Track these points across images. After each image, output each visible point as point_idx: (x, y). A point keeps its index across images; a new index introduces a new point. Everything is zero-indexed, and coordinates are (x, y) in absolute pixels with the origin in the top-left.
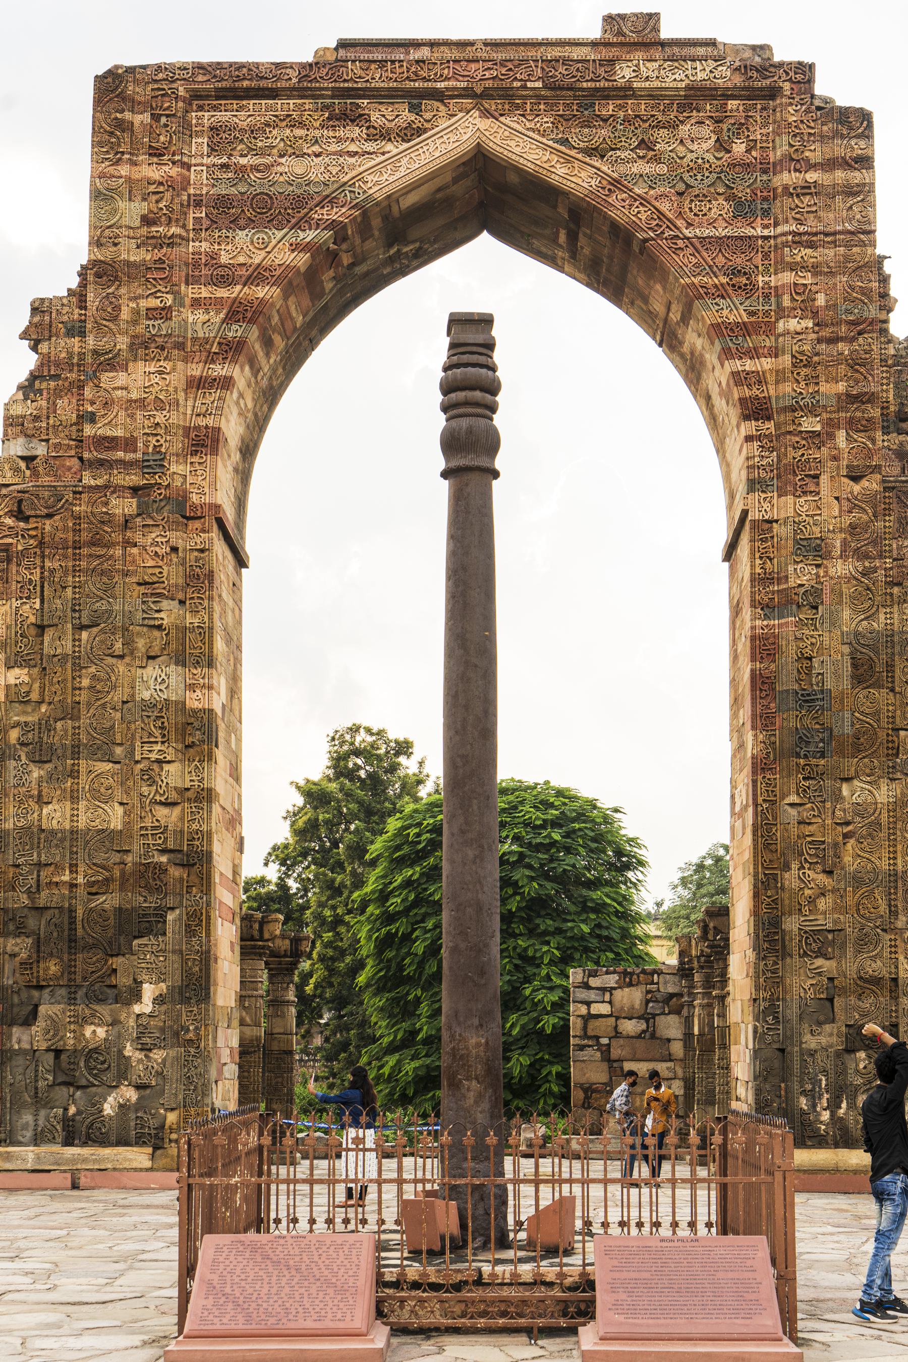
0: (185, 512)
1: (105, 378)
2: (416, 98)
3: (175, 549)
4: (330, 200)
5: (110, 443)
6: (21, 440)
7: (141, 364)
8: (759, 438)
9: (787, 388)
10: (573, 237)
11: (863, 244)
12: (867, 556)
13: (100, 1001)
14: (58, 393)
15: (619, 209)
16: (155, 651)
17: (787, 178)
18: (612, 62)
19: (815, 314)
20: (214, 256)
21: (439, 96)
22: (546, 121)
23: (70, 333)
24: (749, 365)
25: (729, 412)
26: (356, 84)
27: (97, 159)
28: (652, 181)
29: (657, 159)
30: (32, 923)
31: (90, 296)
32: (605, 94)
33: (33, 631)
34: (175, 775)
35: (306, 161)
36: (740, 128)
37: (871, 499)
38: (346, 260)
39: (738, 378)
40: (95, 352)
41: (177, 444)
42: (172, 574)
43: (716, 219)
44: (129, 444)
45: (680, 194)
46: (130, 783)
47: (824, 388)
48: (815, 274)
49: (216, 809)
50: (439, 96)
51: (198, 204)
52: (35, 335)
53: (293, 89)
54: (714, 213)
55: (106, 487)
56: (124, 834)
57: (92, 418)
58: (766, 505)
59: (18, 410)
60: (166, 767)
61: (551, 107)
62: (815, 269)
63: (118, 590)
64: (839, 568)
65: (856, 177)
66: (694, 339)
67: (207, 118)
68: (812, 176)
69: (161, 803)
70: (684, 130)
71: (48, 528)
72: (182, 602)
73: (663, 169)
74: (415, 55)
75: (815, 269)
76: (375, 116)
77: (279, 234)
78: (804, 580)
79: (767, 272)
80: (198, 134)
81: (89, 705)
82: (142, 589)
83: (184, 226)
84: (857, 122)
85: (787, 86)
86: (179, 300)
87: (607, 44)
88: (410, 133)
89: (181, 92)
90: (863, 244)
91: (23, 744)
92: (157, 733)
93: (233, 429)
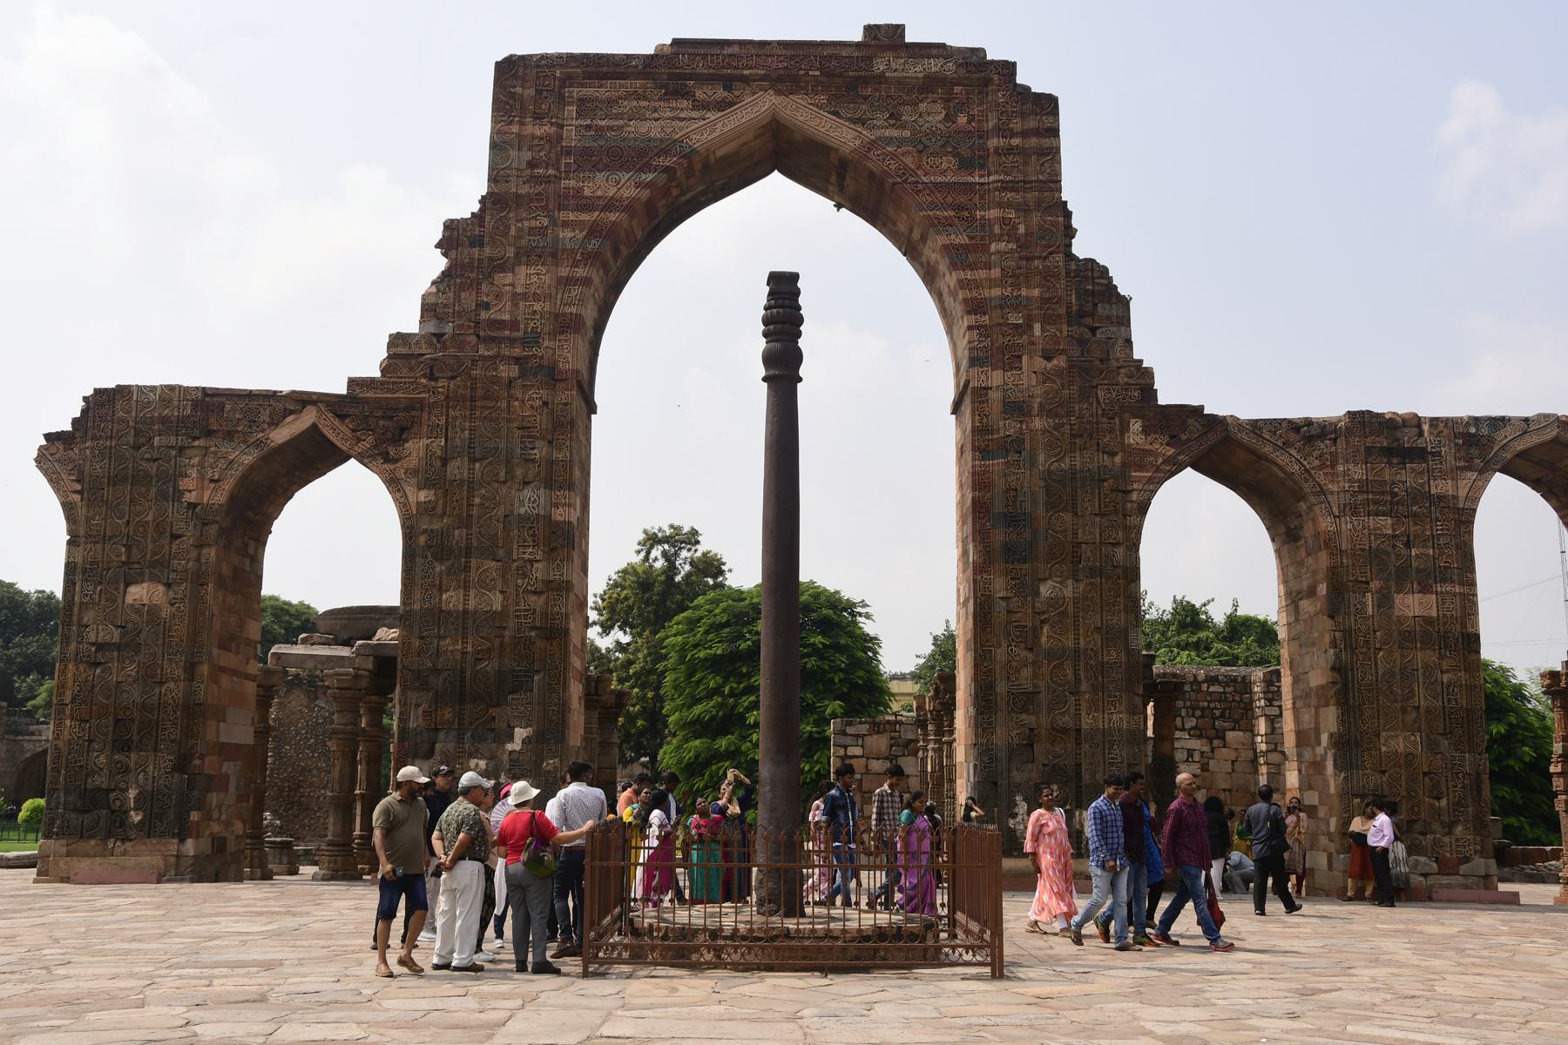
0: (553, 376)
2: (728, 82)
3: (545, 403)
4: (665, 152)
5: (500, 324)
6: (434, 321)
7: (523, 268)
8: (978, 327)
9: (996, 292)
10: (841, 178)
12: (1057, 415)
14: (462, 287)
16: (530, 478)
18: (870, 59)
20: (579, 190)
21: (746, 80)
22: (823, 99)
23: (472, 245)
24: (969, 275)
25: (957, 309)
27: (495, 121)
28: (900, 142)
31: (488, 218)
32: (866, 81)
34: (539, 571)
35: (648, 123)
36: (961, 107)
37: (1059, 372)
38: (675, 192)
39: (963, 284)
40: (491, 259)
42: (542, 421)
43: (946, 170)
44: (514, 325)
45: (920, 152)
48: (1017, 210)
49: (572, 597)
50: (746, 80)
51: (568, 153)
52: (445, 245)
55: (496, 357)
56: (503, 614)
57: (487, 306)
58: (983, 377)
59: (432, 300)
62: (1018, 208)
64: (1037, 423)
65: (1046, 142)
66: (932, 253)
68: (1016, 141)
70: (923, 107)
72: (550, 442)
73: (907, 133)
76: (699, 94)
79: (982, 208)
80: (570, 104)
81: (479, 517)
82: (521, 432)
83: (558, 169)
84: (1048, 104)
85: (996, 77)
86: (554, 222)
88: (722, 106)
91: (430, 547)
93: (590, 314)
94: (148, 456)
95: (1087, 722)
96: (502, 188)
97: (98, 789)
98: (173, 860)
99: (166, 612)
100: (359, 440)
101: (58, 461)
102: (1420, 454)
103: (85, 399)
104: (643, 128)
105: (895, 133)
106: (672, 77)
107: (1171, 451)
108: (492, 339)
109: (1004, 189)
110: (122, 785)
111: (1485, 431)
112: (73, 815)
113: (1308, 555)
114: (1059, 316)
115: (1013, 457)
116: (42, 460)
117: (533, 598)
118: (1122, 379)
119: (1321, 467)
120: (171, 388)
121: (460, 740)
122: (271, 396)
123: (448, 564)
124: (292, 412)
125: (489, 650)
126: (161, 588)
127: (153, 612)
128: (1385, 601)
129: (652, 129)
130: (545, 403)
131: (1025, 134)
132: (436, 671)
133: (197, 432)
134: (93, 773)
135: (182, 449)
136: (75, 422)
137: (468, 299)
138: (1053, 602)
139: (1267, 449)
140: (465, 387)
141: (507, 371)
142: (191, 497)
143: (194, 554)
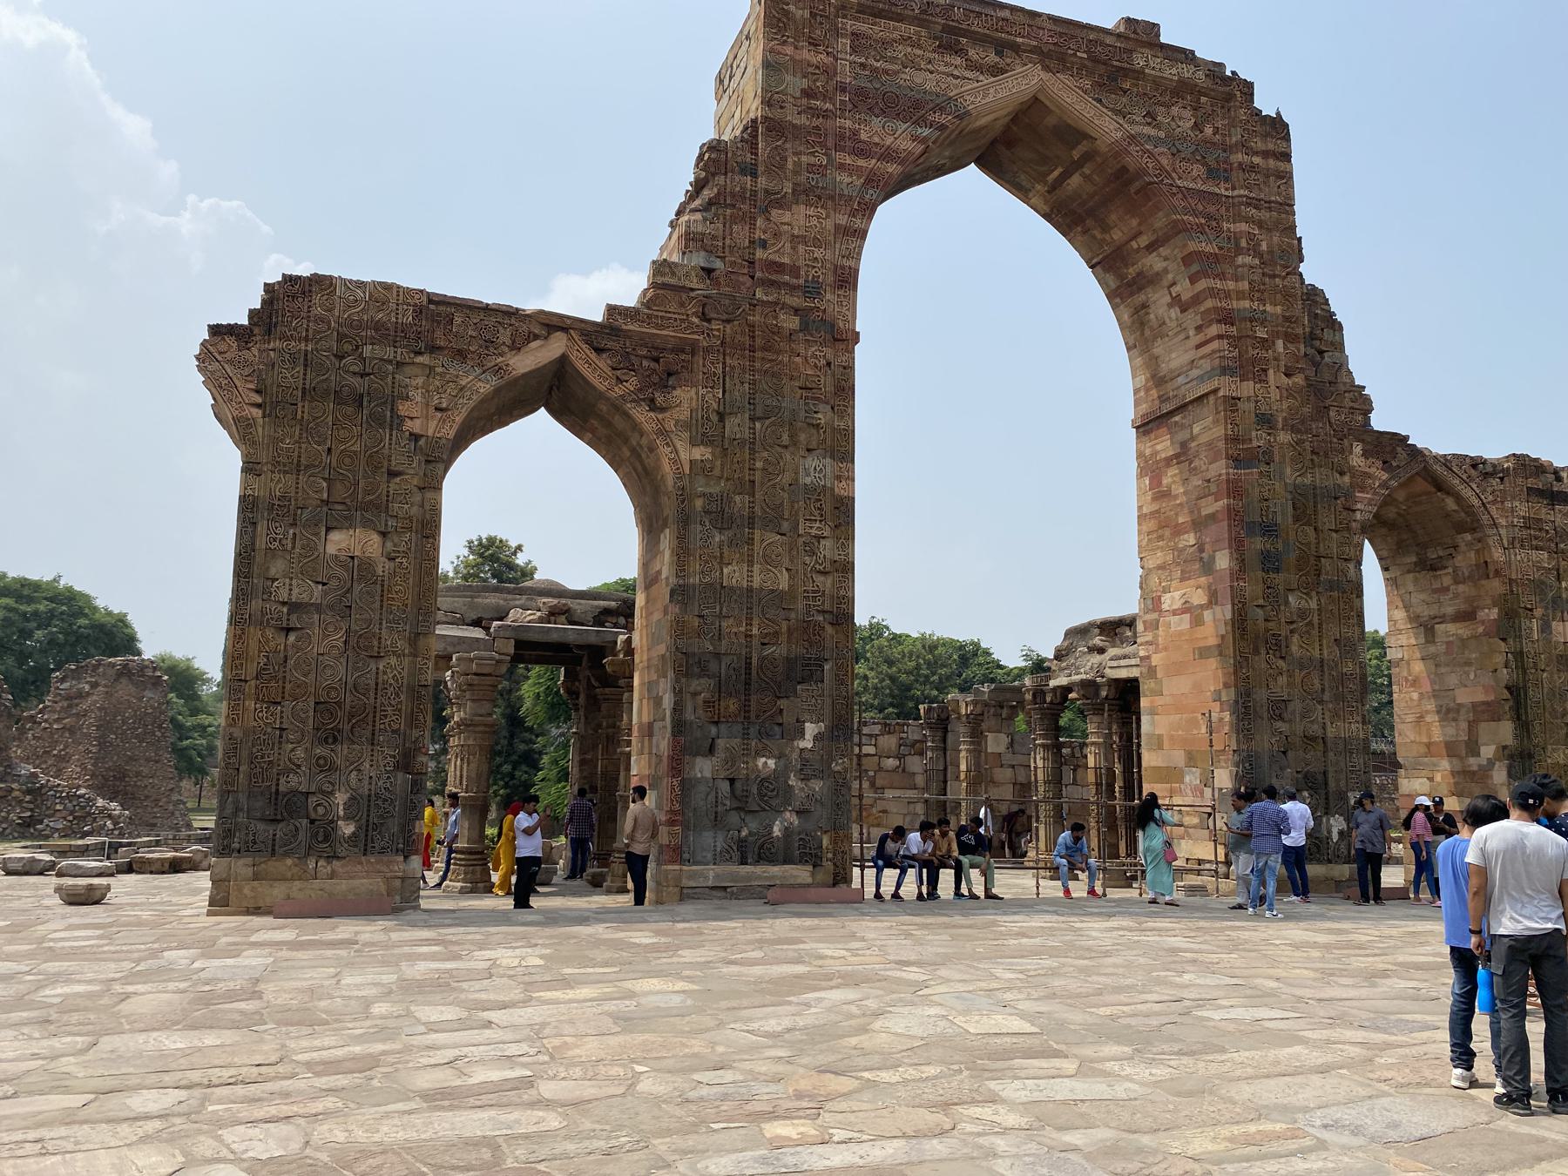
1: (774, 212)
2: (1001, 47)
5: (779, 267)
6: (703, 253)
8: (1228, 337)
9: (1246, 304)
11: (1287, 213)
12: (1299, 431)
14: (734, 220)
16: (814, 445)
17: (1239, 157)
18: (1131, 51)
19: (1261, 256)
20: (855, 133)
21: (1016, 49)
22: (1087, 84)
23: (743, 172)
28: (1157, 142)
29: (1158, 127)
30: (713, 666)
33: (714, 418)
36: (1208, 117)
41: (830, 279)
43: (1193, 177)
44: (794, 271)
47: (1268, 308)
48: (1260, 227)
50: (1016, 49)
51: (843, 90)
53: (916, 18)
54: (1195, 173)
55: (776, 304)
57: (764, 244)
60: (823, 542)
61: (1091, 73)
63: (786, 390)
64: (1284, 437)
65: (1282, 165)
67: (849, 25)
68: (1257, 160)
69: (819, 572)
70: (1175, 110)
71: (728, 330)
73: (1162, 134)
74: (1001, 14)
76: (971, 52)
78: (1261, 443)
88: (996, 71)
90: (1287, 213)
92: (816, 513)
94: (354, 368)
95: (1331, 732)
96: (776, 114)
97: (294, 792)
98: (398, 883)
99: (382, 567)
101: (230, 362)
104: (919, 78)
105: (1147, 130)
107: (1385, 476)
108: (773, 283)
112: (261, 826)
113: (1457, 582)
115: (1264, 468)
116: (206, 358)
117: (819, 579)
118: (1347, 403)
119: (1494, 502)
120: (388, 287)
121: (746, 735)
122: (511, 313)
123: (730, 533)
124: (536, 337)
125: (776, 634)
126: (376, 538)
127: (358, 568)
128: (1546, 628)
129: (927, 81)
130: (829, 364)
131: (1266, 154)
132: (717, 655)
134: (287, 772)
135: (399, 365)
136: (253, 314)
137: (741, 233)
138: (1303, 614)
140: (743, 333)
141: (790, 322)
142: (415, 426)
143: (417, 498)
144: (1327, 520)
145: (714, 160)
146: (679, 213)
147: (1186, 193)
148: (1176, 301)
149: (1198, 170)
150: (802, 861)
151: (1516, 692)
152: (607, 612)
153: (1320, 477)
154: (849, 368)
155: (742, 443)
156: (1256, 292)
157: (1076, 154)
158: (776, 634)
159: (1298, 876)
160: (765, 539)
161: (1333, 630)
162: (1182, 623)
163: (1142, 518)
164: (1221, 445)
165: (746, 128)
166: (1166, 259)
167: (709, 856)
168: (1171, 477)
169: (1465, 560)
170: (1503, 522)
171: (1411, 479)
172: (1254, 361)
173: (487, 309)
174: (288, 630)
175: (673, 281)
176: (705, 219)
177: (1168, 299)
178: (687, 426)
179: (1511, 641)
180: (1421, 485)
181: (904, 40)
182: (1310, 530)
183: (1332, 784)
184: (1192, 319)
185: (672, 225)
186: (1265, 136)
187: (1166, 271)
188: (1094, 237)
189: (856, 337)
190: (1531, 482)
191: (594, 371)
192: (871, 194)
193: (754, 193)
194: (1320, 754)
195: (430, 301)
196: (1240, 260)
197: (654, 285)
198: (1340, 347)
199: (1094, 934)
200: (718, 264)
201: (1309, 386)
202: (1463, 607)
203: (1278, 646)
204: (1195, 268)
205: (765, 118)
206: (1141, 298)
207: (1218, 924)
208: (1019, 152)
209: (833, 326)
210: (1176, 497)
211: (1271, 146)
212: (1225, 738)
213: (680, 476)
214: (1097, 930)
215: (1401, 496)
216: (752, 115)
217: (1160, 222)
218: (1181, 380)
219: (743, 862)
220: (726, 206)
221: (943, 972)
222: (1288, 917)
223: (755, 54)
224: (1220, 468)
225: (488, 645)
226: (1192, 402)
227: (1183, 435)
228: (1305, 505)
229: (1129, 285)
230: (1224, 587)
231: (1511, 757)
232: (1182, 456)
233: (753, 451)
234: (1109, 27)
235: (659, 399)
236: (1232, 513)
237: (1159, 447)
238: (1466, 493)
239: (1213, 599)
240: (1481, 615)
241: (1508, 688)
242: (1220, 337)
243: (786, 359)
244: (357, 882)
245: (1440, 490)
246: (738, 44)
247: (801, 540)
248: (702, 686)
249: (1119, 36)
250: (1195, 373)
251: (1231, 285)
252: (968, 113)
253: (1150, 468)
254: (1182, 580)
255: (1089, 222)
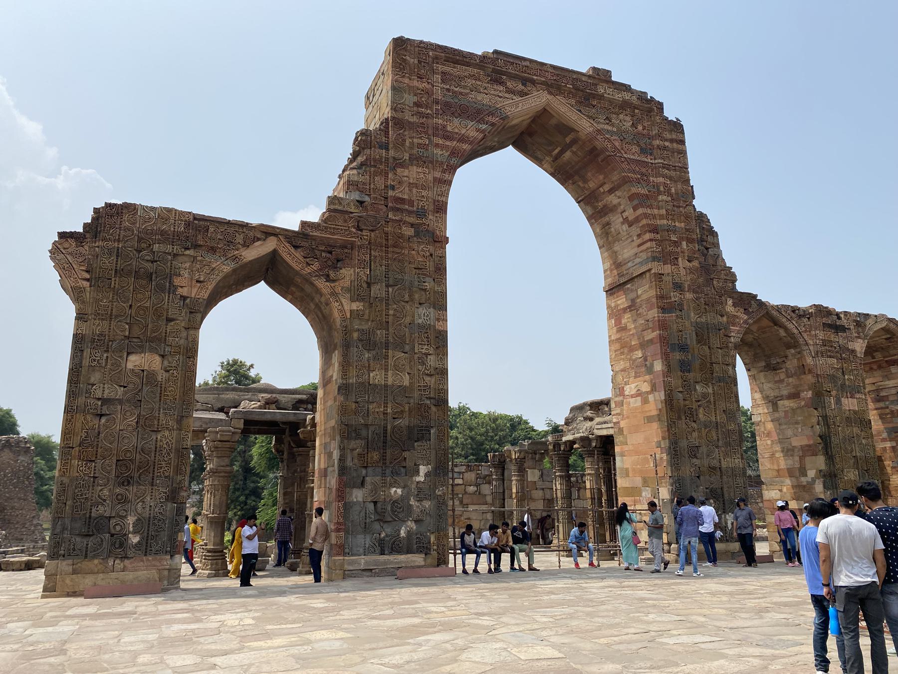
1: (399, 170)
2: (525, 81)
4: (492, 114)
5: (402, 201)
6: (358, 192)
8: (655, 240)
12: (697, 293)
13: (398, 474)
14: (376, 174)
15: (600, 143)
16: (423, 301)
17: (657, 142)
18: (596, 85)
19: (672, 196)
20: (444, 127)
21: (533, 82)
22: (573, 101)
23: (381, 147)
26: (502, 68)
28: (612, 133)
30: (364, 433)
33: (365, 285)
36: (639, 121)
41: (431, 207)
43: (633, 152)
44: (411, 203)
46: (412, 363)
47: (677, 224)
48: (671, 180)
50: (533, 82)
51: (437, 103)
53: (477, 64)
54: (633, 150)
55: (400, 221)
60: (429, 357)
61: (574, 96)
62: (671, 178)
63: (407, 270)
64: (689, 296)
68: (667, 144)
69: (427, 375)
70: (621, 116)
74: (524, 63)
75: (671, 178)
76: (509, 84)
77: (472, 123)
78: (677, 299)
87: (594, 78)
88: (522, 94)
89: (431, 53)
91: (361, 340)
92: (425, 340)
95: (724, 465)
96: (399, 115)
97: (101, 517)
98: (166, 573)
99: (162, 376)
100: (308, 264)
101: (71, 254)
102: (843, 329)
103: (96, 210)
104: (480, 97)
105: (606, 127)
106: (494, 71)
107: (746, 317)
109: (664, 168)
110: (123, 513)
111: (862, 320)
112: (78, 539)
113: (788, 377)
114: (693, 239)
115: (679, 313)
116: (56, 251)
117: (427, 379)
119: (806, 331)
120: (169, 210)
121: (384, 474)
123: (374, 352)
124: (259, 239)
125: (402, 412)
126: (158, 359)
127: (147, 377)
128: (838, 402)
129: (484, 99)
130: (431, 255)
131: (672, 141)
132: (366, 426)
133: (189, 244)
134: (97, 504)
135: (175, 255)
137: (379, 182)
138: (705, 396)
139: (784, 320)
140: (381, 237)
141: (409, 232)
142: (184, 292)
143: (184, 334)
144: (715, 342)
145: (364, 141)
146: (344, 171)
147: (629, 161)
148: (626, 220)
149: (635, 149)
150: (419, 551)
151: (825, 439)
152: (300, 402)
153: (709, 318)
154: (443, 258)
155: (381, 300)
156: (669, 215)
157: (568, 140)
158: (402, 412)
159: (710, 551)
160: (396, 356)
161: (722, 405)
162: (636, 402)
163: (611, 342)
164: (654, 300)
165: (382, 123)
166: (619, 197)
167: (361, 550)
168: (626, 319)
169: (792, 364)
170: (811, 342)
171: (759, 320)
172: (670, 253)
173: (229, 223)
174: (101, 416)
175: (340, 208)
176: (359, 174)
177: (621, 219)
178: (349, 290)
179: (820, 410)
180: (766, 322)
181: (471, 76)
182: (706, 348)
183: (726, 496)
184: (635, 230)
185: (340, 177)
186: (671, 131)
187: (619, 204)
188: (579, 186)
189: (446, 240)
190: (824, 320)
191: (293, 258)
192: (454, 161)
193: (387, 159)
194: (718, 477)
195: (195, 219)
196: (660, 198)
197: (329, 210)
198: (717, 245)
199: (594, 590)
200: (367, 199)
201: (701, 267)
202: (793, 391)
203: (692, 415)
204: (636, 202)
205: (393, 118)
206: (606, 219)
207: (666, 582)
208: (535, 139)
209: (433, 234)
210: (630, 330)
211: (674, 137)
212: (664, 469)
213: (344, 319)
214: (595, 588)
215: (754, 328)
216: (386, 116)
217: (615, 177)
218: (630, 264)
219: (382, 553)
220: (371, 166)
221: (504, 619)
222: (707, 576)
223: (387, 83)
224: (654, 313)
225: (228, 423)
226: (637, 276)
227: (632, 295)
228: (702, 334)
229: (599, 212)
230: (660, 380)
231: (824, 476)
232: (633, 307)
233: (387, 304)
234: (584, 71)
235: (332, 275)
236: (663, 340)
237: (619, 302)
238: (790, 326)
239: (654, 388)
240: (803, 395)
241: (820, 436)
242: (651, 240)
243: (406, 252)
244: (140, 573)
245: (776, 325)
246: (377, 77)
247: (416, 356)
248: (357, 445)
249: (589, 76)
250: (638, 260)
251: (656, 211)
252: (507, 117)
253: (615, 314)
254: (635, 377)
255: (576, 178)
